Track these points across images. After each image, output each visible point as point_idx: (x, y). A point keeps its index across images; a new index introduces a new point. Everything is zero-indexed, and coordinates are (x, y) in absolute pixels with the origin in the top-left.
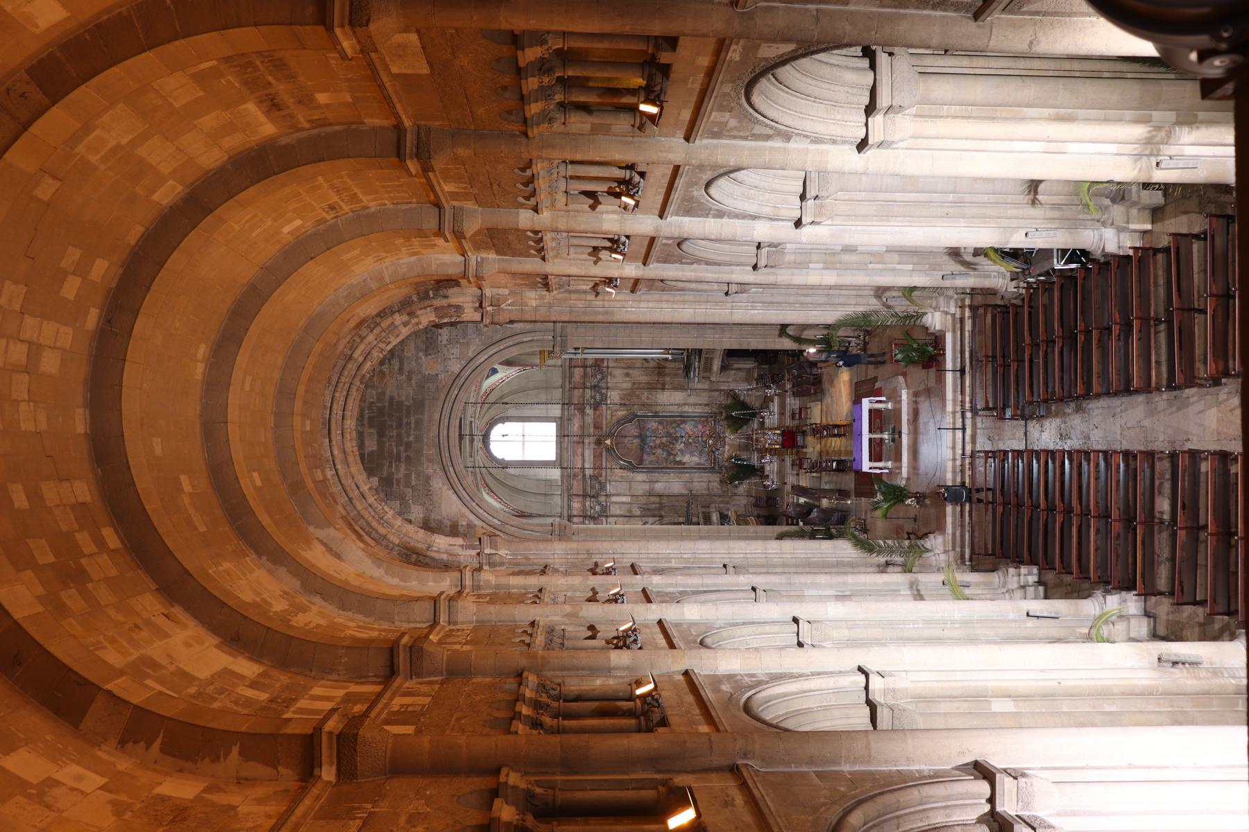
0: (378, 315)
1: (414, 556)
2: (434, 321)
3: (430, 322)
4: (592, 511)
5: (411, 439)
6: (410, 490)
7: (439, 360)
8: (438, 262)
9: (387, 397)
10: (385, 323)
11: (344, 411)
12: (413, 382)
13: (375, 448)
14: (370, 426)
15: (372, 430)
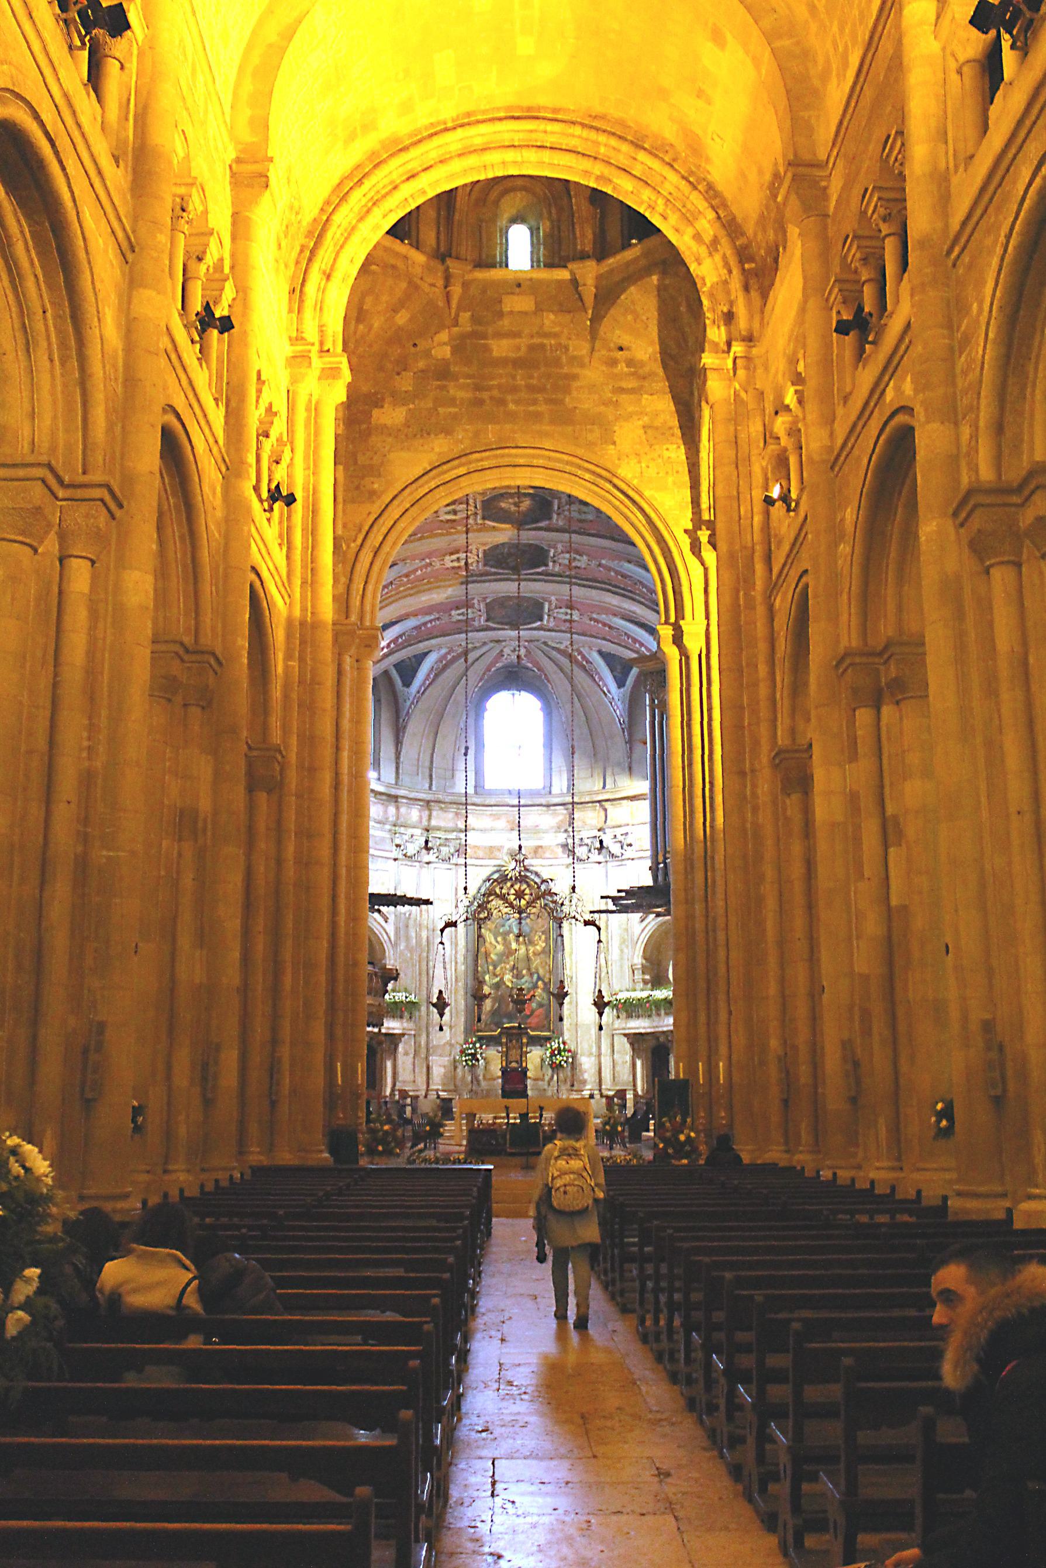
0: (710, 187)
1: (312, 244)
2: (705, 284)
3: (703, 279)
4: (406, 837)
5: (512, 407)
6: (430, 405)
7: (638, 447)
8: (813, 121)
9: (576, 370)
10: (697, 201)
11: (551, 148)
12: (602, 408)
13: (495, 354)
14: (531, 348)
15: (523, 349)
